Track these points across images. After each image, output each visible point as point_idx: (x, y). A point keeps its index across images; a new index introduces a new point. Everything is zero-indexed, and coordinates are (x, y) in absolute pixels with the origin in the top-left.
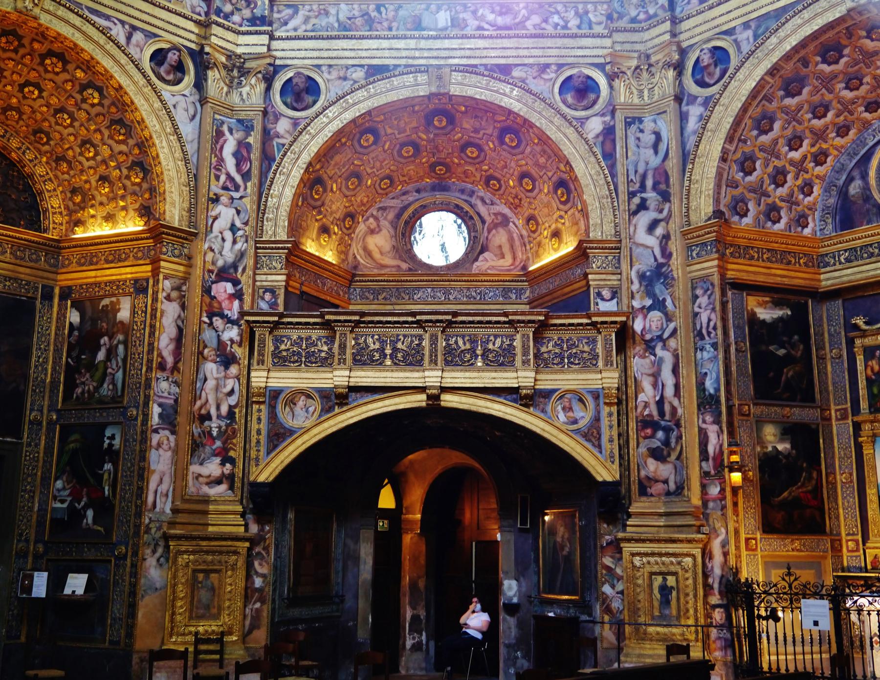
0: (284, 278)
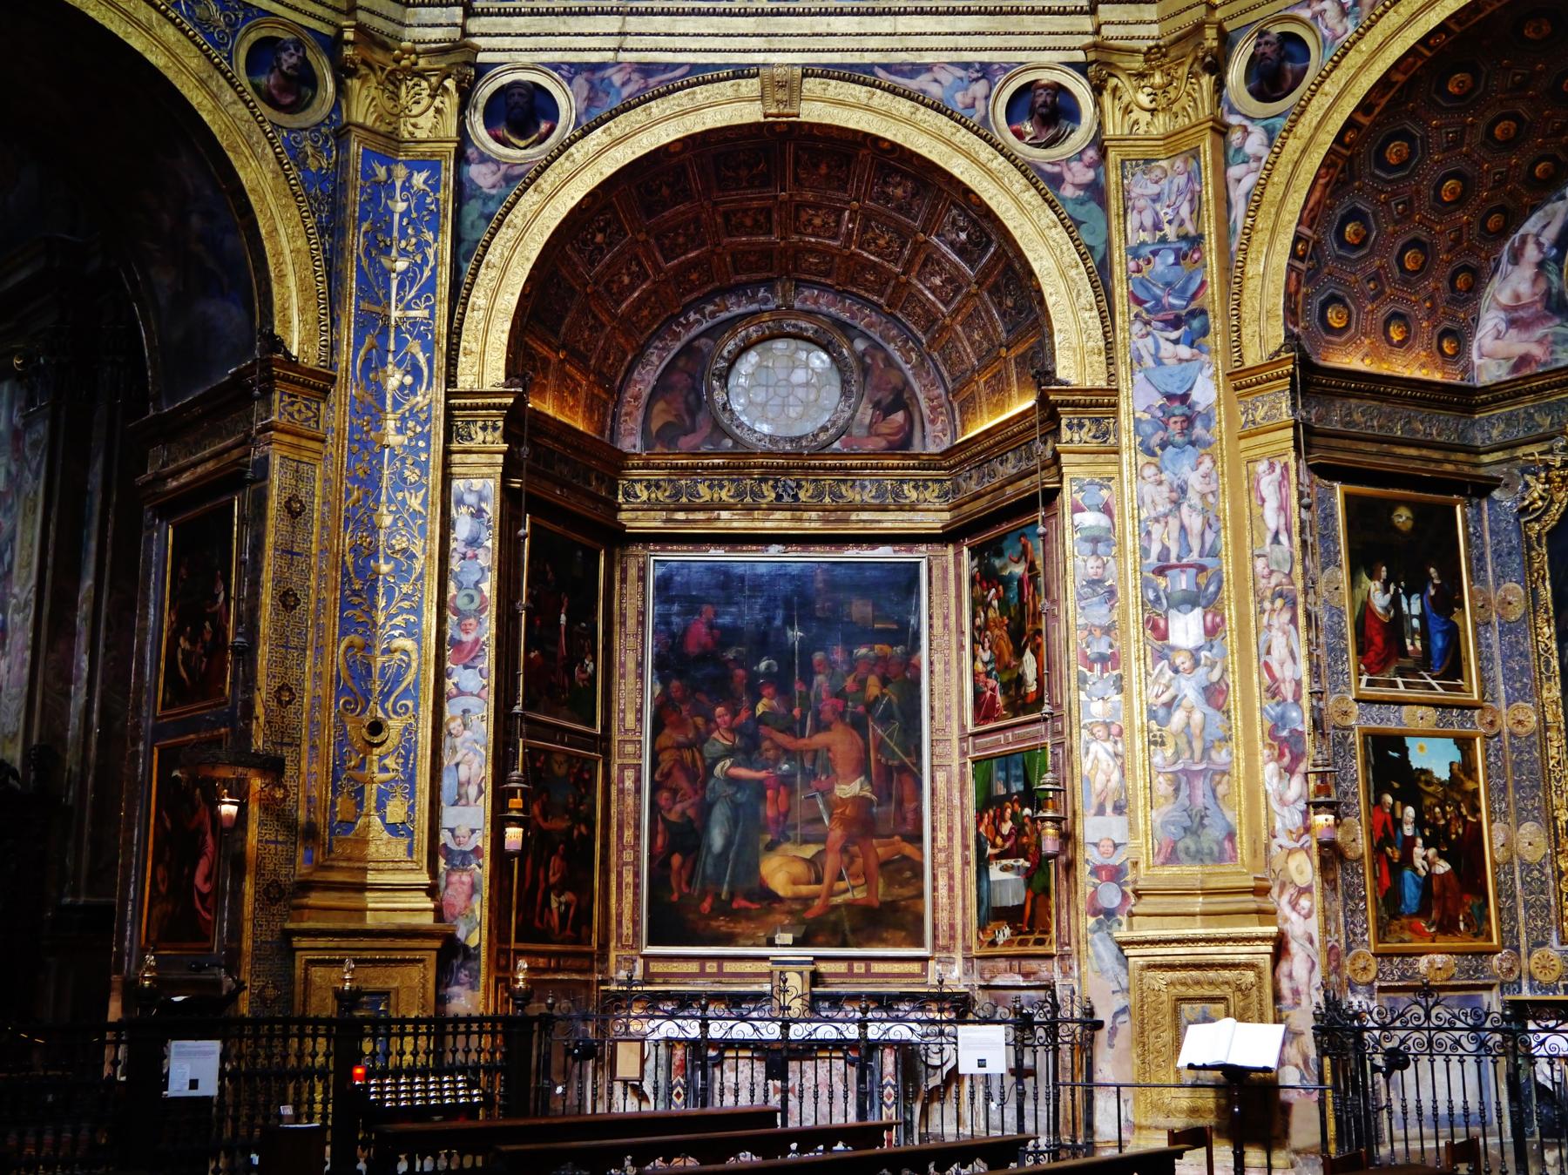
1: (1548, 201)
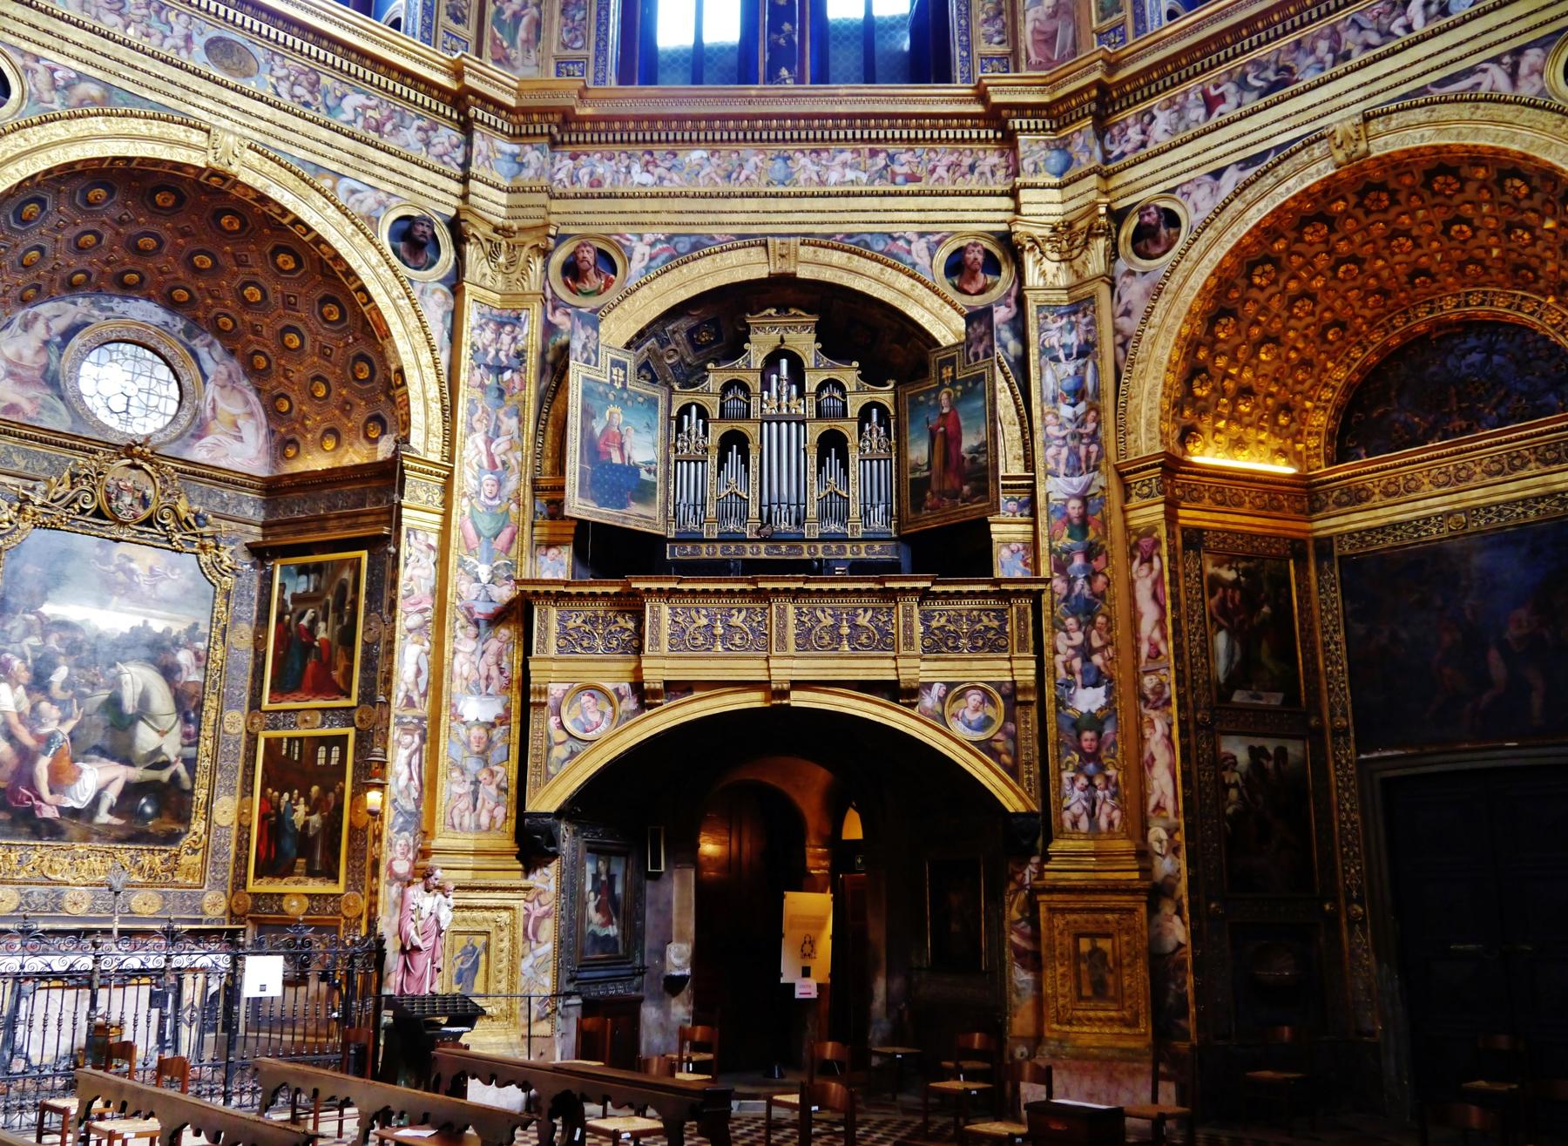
0: (1161, 507)
1: (62, 299)
